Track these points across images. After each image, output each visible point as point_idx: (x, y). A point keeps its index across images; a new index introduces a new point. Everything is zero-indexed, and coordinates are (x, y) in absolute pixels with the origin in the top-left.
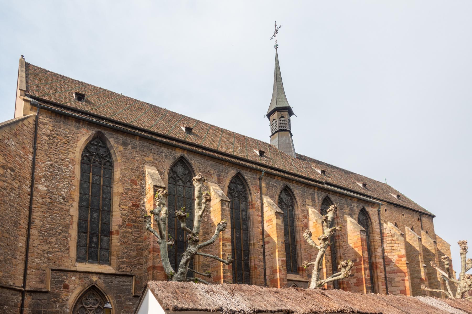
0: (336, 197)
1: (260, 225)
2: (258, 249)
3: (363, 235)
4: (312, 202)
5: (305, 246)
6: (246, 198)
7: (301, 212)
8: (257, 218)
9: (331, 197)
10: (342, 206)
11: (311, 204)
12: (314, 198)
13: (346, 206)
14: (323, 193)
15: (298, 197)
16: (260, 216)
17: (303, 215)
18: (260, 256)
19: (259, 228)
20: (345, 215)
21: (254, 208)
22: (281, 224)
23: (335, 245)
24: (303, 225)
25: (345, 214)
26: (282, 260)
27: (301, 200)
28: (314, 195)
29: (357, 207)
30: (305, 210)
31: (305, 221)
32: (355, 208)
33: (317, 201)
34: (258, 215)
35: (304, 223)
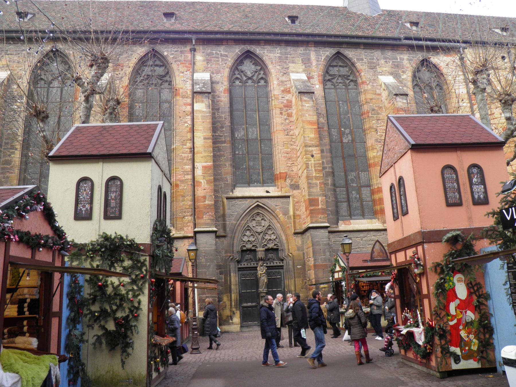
0: (359, 51)
1: (189, 117)
2: (183, 155)
3: (403, 103)
4: (303, 67)
5: (285, 138)
6: (170, 83)
7: (278, 85)
8: (184, 108)
9: (347, 52)
10: (374, 63)
11: (301, 70)
12: (309, 59)
13: (382, 61)
14: (327, 49)
15: (272, 63)
16: (190, 105)
17: (282, 89)
18: (185, 165)
19: (186, 122)
20: (379, 77)
21: (179, 95)
22: (205, 110)
23: (363, 128)
24: (282, 106)
25: (381, 75)
26: (203, 167)
27: (278, 67)
28: (309, 55)
29: (409, 60)
30: (286, 81)
31: (287, 98)
32: (405, 62)
33: (314, 63)
34: (186, 104)
35: (285, 101)
